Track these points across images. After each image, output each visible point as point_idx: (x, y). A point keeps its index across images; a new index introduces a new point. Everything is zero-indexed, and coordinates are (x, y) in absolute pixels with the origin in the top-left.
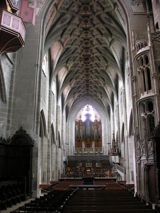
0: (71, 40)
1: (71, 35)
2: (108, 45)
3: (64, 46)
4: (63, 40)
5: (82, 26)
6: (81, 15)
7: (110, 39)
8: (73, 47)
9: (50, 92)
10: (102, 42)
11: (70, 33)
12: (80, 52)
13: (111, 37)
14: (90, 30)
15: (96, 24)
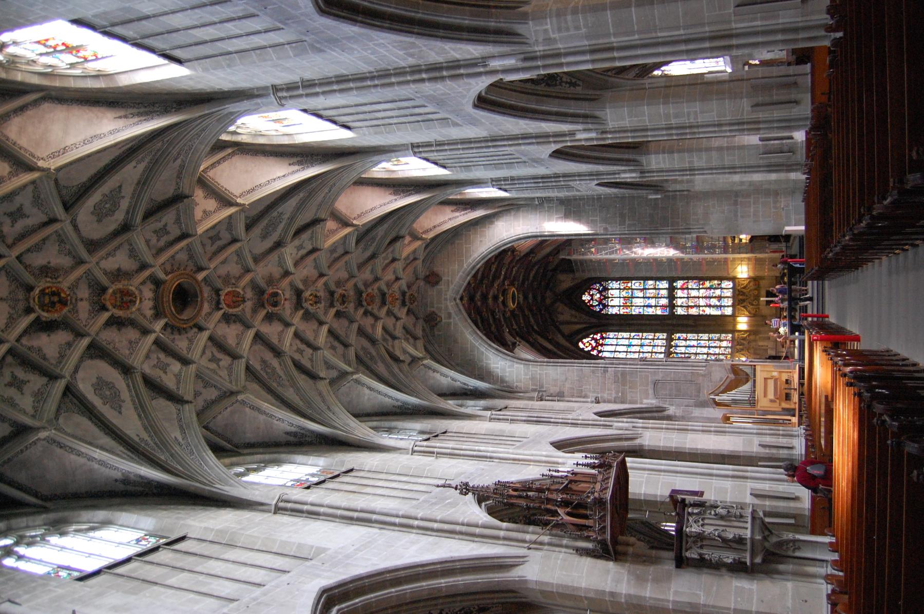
0: (333, 348)
1: (315, 349)
2: (349, 234)
3: (349, 369)
4: (334, 374)
5: (288, 312)
6: (255, 311)
7: (331, 224)
8: (353, 343)
9: (494, 419)
10: (340, 251)
11: (311, 351)
12: (370, 320)
13: (323, 220)
14: (301, 286)
15: (282, 267)
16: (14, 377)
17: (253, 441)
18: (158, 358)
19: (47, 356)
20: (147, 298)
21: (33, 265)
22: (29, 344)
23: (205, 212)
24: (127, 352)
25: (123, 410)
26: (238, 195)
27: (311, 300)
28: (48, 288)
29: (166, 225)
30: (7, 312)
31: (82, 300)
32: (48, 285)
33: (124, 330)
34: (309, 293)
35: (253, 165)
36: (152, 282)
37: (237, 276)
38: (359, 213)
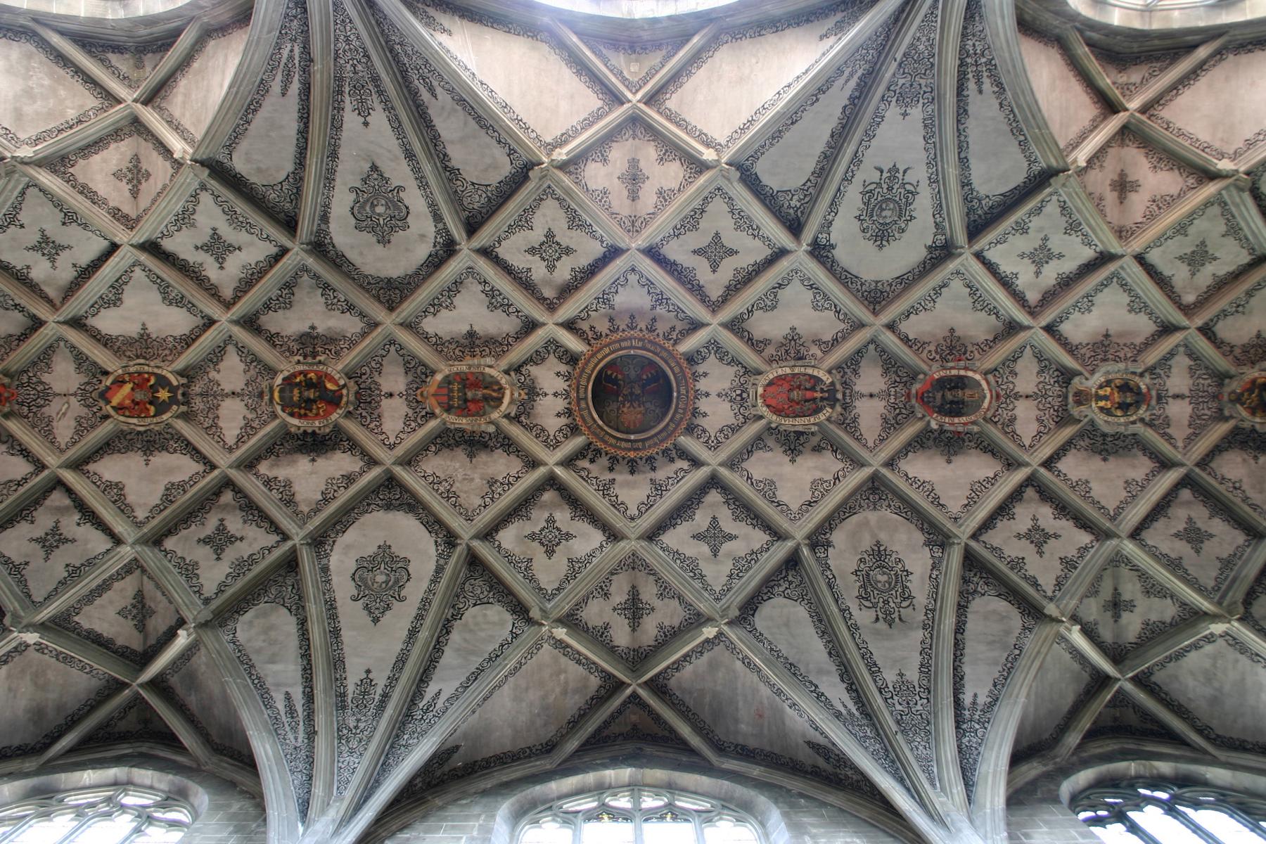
4: (1166, 611)
16: (221, 528)
17: (752, 743)
18: (551, 521)
19: (298, 498)
20: (550, 391)
21: (283, 334)
22: (271, 474)
23: (660, 193)
24: (478, 501)
25: (387, 618)
26: (723, 142)
27: (1105, 398)
28: (301, 373)
29: (550, 235)
30: (241, 417)
31: (391, 395)
32: (300, 368)
33: (483, 457)
34: (1099, 378)
35: (754, 61)
36: (560, 358)
37: (828, 337)
38: (1249, 135)
